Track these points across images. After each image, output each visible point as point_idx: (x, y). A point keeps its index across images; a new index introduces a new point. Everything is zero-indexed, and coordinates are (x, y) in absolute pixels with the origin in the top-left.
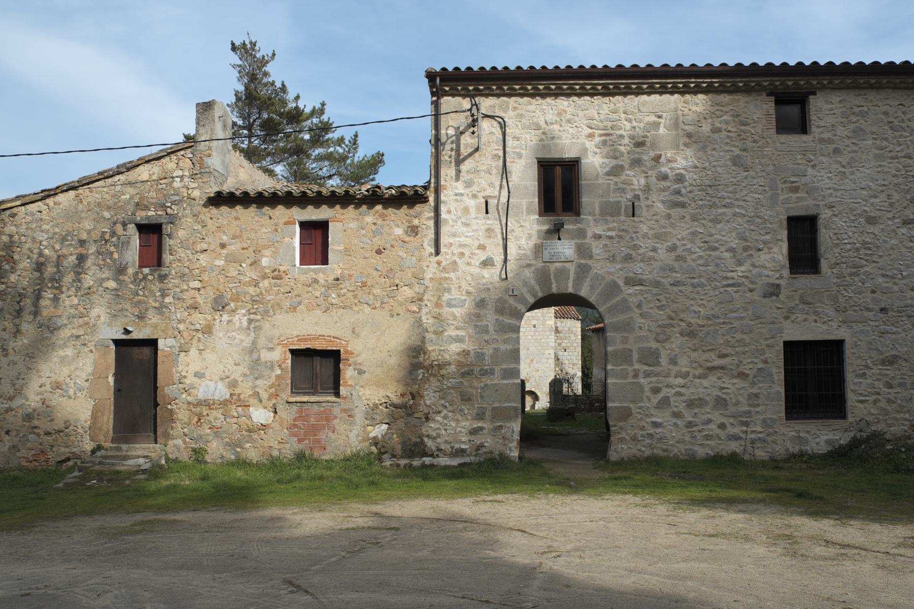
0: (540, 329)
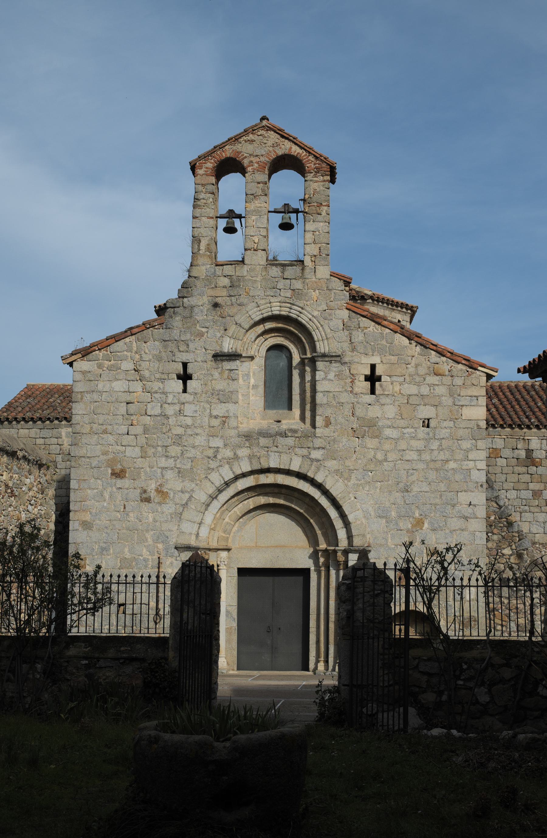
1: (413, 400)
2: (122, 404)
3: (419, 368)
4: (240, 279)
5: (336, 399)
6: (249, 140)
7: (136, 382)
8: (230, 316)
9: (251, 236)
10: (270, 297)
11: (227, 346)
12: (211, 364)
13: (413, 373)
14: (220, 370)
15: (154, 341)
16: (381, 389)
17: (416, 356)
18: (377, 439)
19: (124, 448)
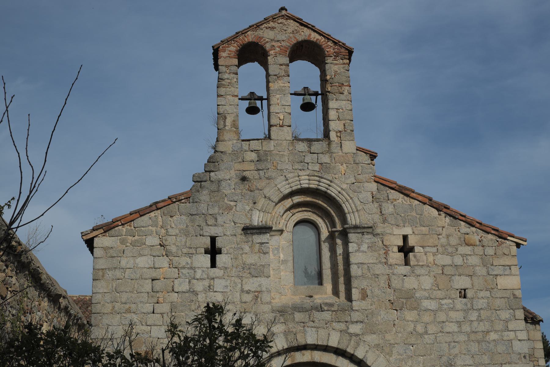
0: (481, 303)
1: (448, 271)
2: (147, 281)
3: (451, 238)
4: (267, 154)
5: (371, 270)
6: (269, 27)
7: (162, 257)
8: (258, 189)
9: (276, 113)
10: (298, 171)
11: (257, 219)
12: (241, 237)
13: (444, 244)
14: (250, 243)
15: (181, 216)
16: (415, 260)
17: (447, 226)
18: (416, 311)
19: (149, 327)
